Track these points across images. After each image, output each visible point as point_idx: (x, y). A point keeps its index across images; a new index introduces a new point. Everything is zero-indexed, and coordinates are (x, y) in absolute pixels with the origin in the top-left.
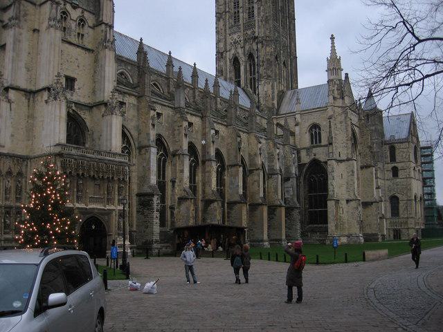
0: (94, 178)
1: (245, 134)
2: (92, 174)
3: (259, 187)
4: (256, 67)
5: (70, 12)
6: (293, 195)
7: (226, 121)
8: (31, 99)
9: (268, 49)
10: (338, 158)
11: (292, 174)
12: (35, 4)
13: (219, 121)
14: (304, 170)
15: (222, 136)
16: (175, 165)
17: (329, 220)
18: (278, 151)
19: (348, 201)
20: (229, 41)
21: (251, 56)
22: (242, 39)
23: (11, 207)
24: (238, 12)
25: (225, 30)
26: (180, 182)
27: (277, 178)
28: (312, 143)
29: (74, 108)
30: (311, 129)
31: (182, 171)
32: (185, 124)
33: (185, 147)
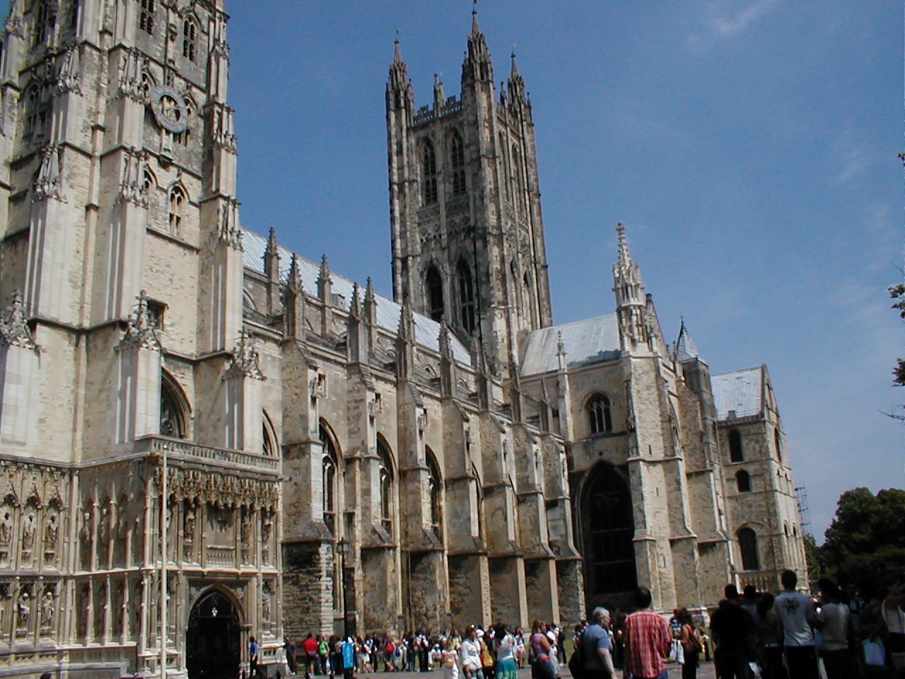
0: (213, 510)
1: (473, 415)
2: (213, 500)
3: (506, 519)
4: (475, 285)
5: (155, 172)
8: (83, 344)
12: (90, 156)
13: (427, 391)
14: (582, 485)
15: (433, 420)
16: (351, 481)
18: (535, 447)
19: (672, 542)
21: (462, 266)
23: (34, 577)
26: (363, 514)
29: (163, 364)
30: (589, 405)
31: (367, 492)
32: (370, 396)
33: (372, 443)
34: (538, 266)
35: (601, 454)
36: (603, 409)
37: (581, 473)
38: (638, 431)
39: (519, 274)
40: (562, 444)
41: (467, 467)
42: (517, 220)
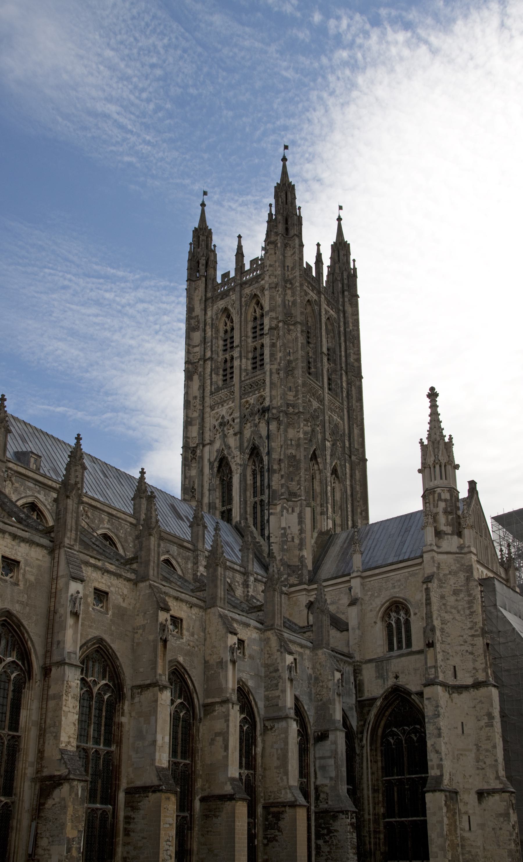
1: (195, 610)
3: (226, 748)
6: (337, 776)
7: (134, 571)
9: (291, 433)
10: (451, 681)
11: (334, 722)
15: (118, 607)
17: (433, 848)
18: (289, 659)
19: (481, 795)
20: (210, 421)
22: (237, 414)
24: (232, 358)
25: (203, 397)
27: (286, 731)
28: (391, 648)
30: (387, 613)
34: (353, 457)
35: (397, 677)
36: (402, 620)
37: (374, 699)
38: (438, 645)
39: (325, 463)
40: (349, 664)
41: (160, 671)
42: (326, 403)
